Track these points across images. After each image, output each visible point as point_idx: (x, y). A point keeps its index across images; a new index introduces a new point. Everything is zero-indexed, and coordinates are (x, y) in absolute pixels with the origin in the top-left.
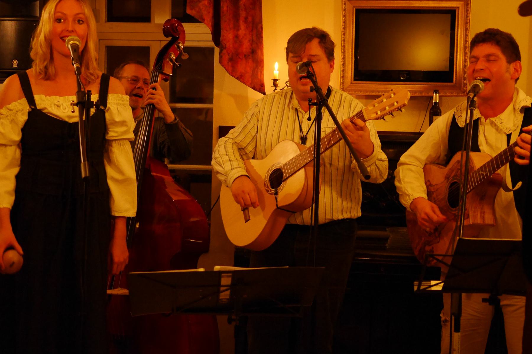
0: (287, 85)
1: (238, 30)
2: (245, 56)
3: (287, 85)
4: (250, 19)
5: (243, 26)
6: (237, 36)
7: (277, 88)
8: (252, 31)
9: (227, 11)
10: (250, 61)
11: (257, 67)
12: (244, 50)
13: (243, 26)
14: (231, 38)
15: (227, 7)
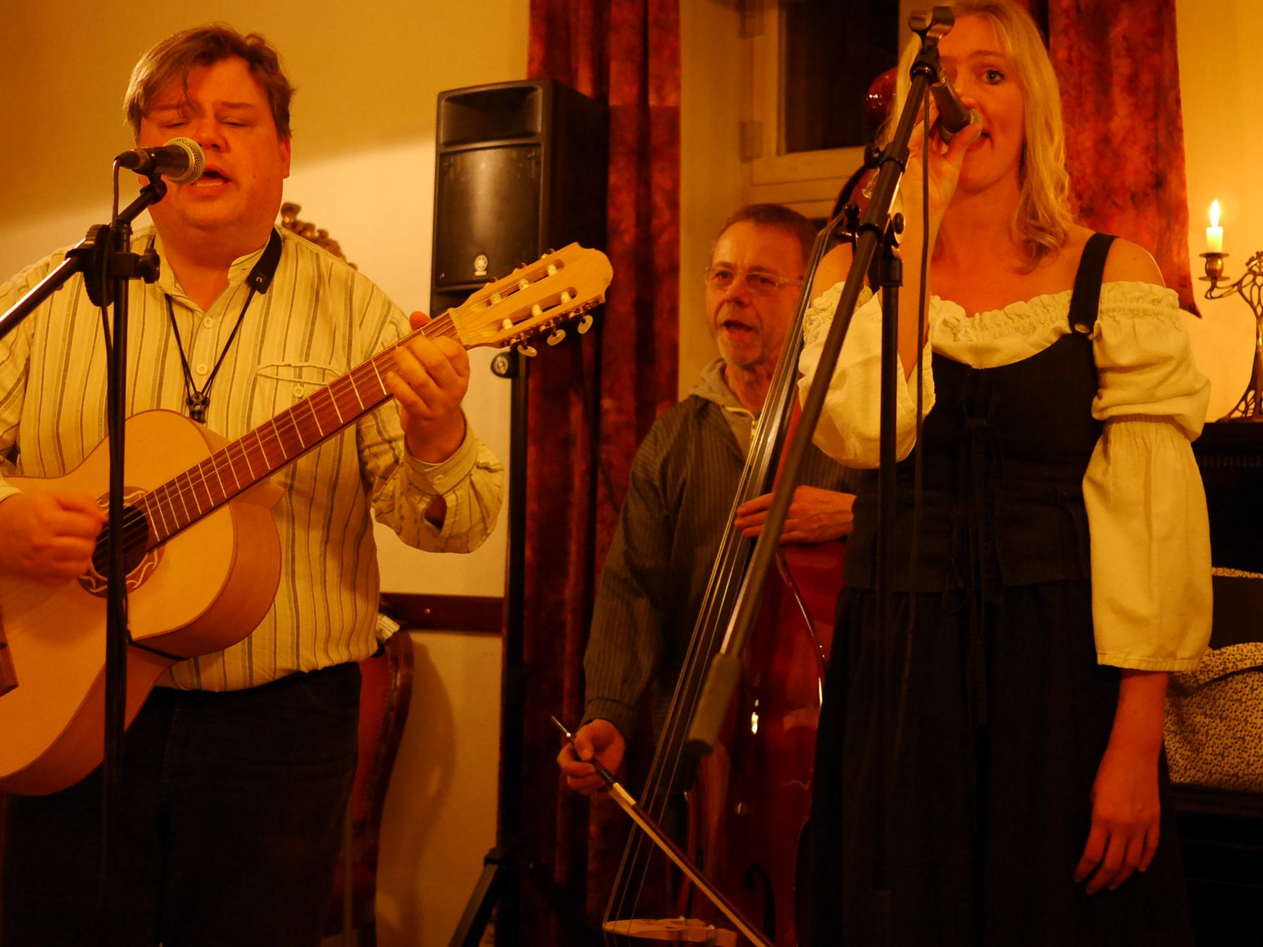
0: (1251, 271)
1: (1109, 119)
2: (1133, 197)
3: (1251, 271)
4: (1146, 79)
5: (1122, 106)
6: (1105, 139)
7: (1219, 284)
8: (1155, 117)
9: (1070, 62)
10: (1151, 212)
11: (1169, 227)
12: (1130, 180)
13: (1122, 106)
14: (1088, 144)
15: (1070, 48)
